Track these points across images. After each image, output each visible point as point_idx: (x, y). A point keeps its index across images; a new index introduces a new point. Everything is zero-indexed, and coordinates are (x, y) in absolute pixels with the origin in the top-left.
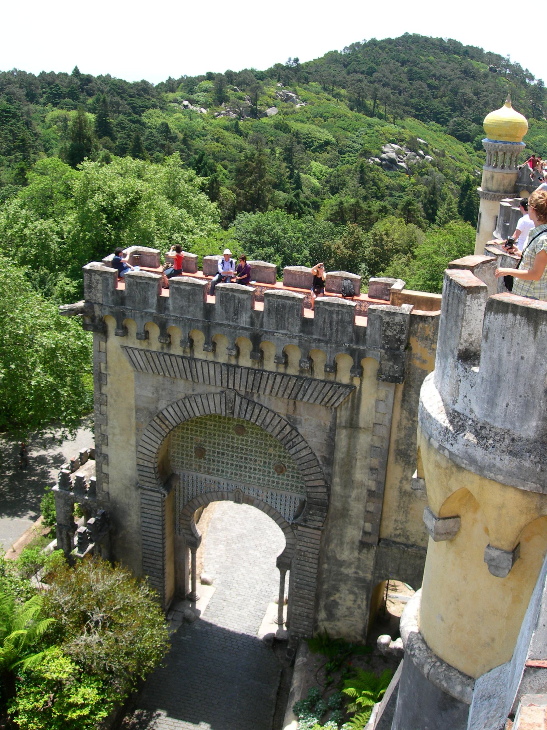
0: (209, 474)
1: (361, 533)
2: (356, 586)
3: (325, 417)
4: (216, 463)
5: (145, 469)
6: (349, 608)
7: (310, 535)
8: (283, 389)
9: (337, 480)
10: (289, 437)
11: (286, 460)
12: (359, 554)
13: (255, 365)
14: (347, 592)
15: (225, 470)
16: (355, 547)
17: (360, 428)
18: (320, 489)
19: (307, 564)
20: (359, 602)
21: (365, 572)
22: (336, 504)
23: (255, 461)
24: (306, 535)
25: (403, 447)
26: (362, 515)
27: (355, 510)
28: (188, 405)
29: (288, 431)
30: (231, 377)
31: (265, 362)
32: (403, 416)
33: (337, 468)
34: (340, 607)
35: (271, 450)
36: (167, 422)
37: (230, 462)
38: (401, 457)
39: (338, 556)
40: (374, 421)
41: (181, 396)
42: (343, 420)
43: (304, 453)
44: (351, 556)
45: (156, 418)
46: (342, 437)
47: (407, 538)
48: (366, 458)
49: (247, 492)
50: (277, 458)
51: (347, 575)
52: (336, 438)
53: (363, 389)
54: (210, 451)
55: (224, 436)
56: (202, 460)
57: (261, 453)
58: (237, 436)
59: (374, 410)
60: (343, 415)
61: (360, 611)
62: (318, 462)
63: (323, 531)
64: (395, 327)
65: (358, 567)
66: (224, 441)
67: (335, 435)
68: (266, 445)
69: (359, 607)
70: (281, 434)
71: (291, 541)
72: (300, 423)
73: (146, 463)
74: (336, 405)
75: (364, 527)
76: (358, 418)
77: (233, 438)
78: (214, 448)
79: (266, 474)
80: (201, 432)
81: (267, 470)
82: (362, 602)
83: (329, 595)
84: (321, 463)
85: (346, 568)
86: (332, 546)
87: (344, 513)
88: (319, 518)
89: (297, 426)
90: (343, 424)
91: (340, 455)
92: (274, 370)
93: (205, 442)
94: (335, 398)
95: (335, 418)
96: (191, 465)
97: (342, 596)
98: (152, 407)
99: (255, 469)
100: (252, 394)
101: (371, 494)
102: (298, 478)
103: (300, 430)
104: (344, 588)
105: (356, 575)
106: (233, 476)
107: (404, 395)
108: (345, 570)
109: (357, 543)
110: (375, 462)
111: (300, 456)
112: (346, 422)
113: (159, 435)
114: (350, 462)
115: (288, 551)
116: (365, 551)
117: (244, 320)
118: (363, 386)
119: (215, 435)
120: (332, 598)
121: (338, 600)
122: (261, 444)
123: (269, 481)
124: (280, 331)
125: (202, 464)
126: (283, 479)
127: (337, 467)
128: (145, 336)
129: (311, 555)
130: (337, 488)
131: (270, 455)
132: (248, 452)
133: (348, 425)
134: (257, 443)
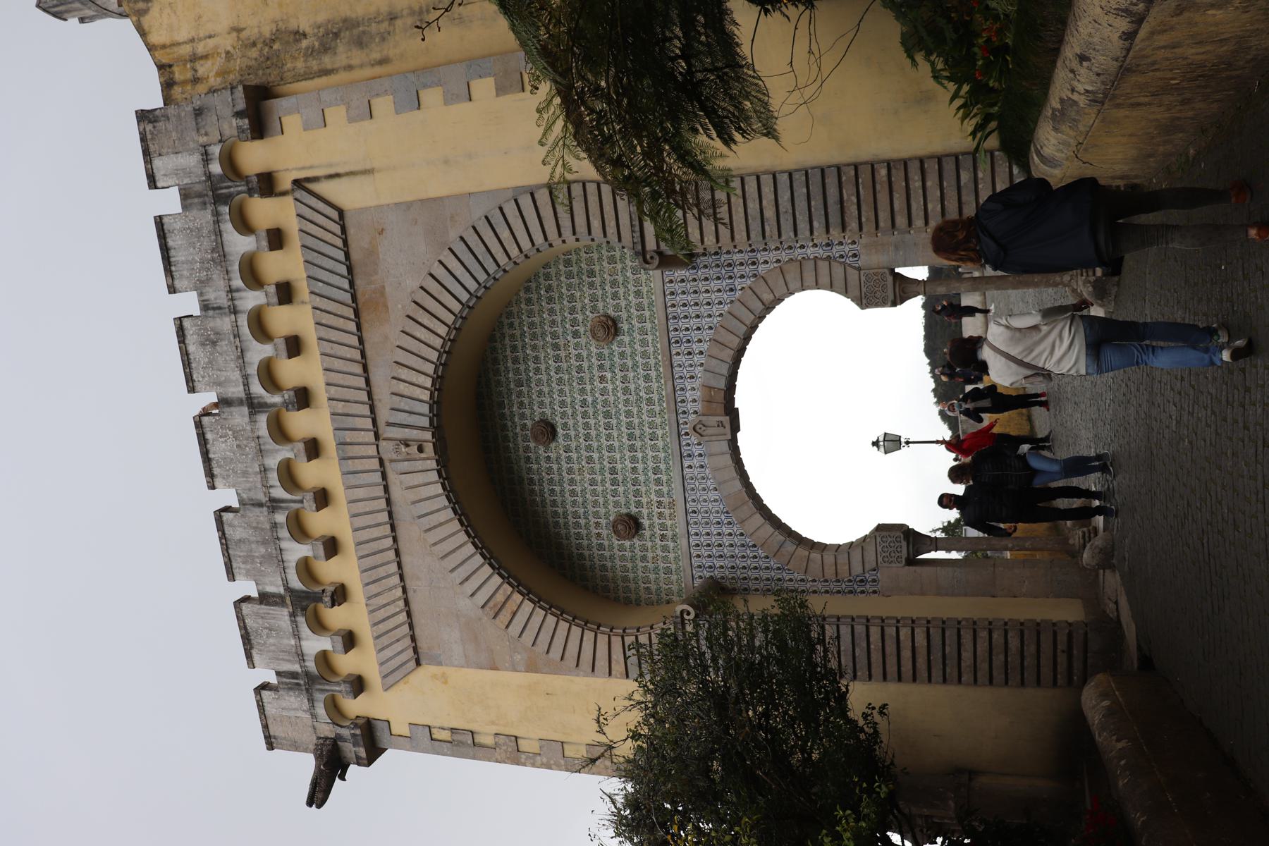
0: (672, 504)
36: (500, 598)
49: (690, 407)
50: (583, 341)
54: (617, 504)
56: (646, 522)
58: (561, 440)
74: (335, 215)
79: (629, 363)
80: (577, 525)
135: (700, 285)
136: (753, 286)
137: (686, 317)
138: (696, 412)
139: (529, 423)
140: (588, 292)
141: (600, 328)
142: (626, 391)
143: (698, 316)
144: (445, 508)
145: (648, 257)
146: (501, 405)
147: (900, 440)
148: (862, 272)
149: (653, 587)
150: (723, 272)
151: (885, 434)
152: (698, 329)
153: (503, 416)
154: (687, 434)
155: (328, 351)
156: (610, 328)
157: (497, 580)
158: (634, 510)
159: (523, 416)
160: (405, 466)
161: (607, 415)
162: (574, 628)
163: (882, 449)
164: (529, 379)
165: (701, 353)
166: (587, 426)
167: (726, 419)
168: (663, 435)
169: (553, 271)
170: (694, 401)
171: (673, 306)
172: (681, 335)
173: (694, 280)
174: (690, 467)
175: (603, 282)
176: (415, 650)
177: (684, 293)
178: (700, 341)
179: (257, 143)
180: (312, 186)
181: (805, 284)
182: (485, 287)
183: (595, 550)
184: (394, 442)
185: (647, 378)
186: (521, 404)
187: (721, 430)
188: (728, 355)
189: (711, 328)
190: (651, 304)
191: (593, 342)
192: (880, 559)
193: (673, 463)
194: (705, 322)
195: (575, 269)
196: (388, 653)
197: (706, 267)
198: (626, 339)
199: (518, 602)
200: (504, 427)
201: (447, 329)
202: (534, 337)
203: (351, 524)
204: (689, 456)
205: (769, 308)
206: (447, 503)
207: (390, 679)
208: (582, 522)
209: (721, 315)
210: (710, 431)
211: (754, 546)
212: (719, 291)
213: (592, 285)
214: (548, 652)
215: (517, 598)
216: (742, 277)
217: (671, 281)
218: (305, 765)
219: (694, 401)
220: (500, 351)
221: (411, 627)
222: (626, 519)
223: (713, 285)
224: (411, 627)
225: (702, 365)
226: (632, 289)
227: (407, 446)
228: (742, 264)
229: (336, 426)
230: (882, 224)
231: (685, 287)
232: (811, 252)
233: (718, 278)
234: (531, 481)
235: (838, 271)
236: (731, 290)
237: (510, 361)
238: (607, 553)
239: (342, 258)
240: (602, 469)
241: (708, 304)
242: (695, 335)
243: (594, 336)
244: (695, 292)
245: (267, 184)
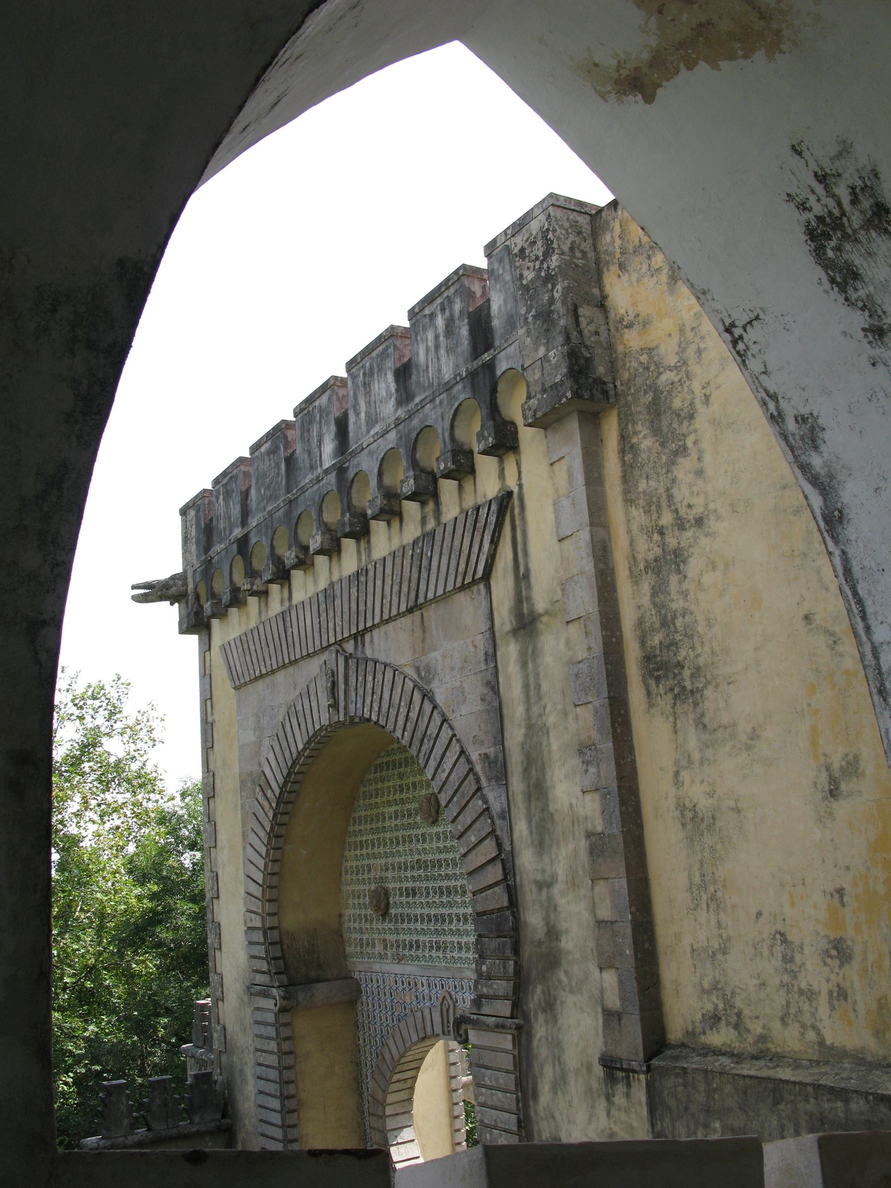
17: (540, 615)
38: (658, 679)
47: (738, 1025)
91: (515, 735)
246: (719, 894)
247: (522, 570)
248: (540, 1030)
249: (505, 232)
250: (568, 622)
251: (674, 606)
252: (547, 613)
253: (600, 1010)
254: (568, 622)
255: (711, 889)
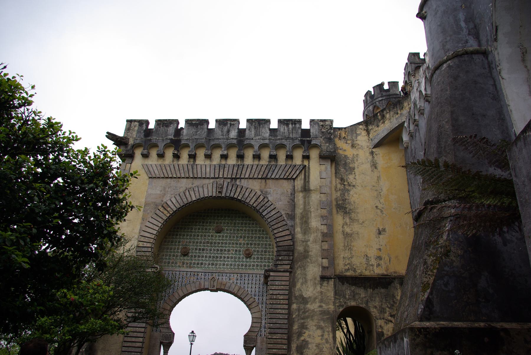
0: (190, 267)
1: (321, 269)
2: (323, 319)
3: (286, 186)
4: (197, 258)
5: (144, 249)
6: (318, 346)
7: (280, 278)
8: (258, 172)
9: (298, 229)
10: (262, 203)
11: (253, 246)
12: (321, 288)
13: (238, 162)
14: (315, 328)
15: (204, 262)
16: (317, 282)
17: (311, 190)
18: (287, 238)
19: (279, 306)
20: (326, 336)
21: (327, 304)
22: (300, 248)
23: (229, 251)
24: (277, 278)
25: (341, 202)
26: (320, 254)
27: (314, 251)
28: (187, 193)
29: (261, 199)
30: (222, 170)
31: (245, 159)
32: (337, 182)
33: (298, 221)
34: (310, 346)
35: (241, 241)
36: (169, 209)
37: (208, 255)
38: (340, 209)
39: (304, 294)
40: (320, 184)
41: (182, 190)
42: (300, 187)
43: (273, 213)
44: (314, 292)
45: (160, 207)
46: (300, 198)
47: (355, 271)
48: (318, 210)
50: (245, 246)
51: (313, 311)
52: (295, 200)
53: (310, 166)
55: (205, 236)
56: (185, 258)
57: (233, 244)
59: (319, 178)
60: (299, 183)
61: (328, 346)
62: (284, 218)
63: (291, 272)
64: (326, 127)
65: (321, 301)
66: (205, 239)
67: (294, 197)
68: (237, 237)
69: (327, 342)
70: (256, 202)
71: (257, 315)
72: (270, 193)
73: (145, 245)
74: (294, 177)
75: (322, 263)
76: (309, 184)
77: (212, 236)
78: (197, 246)
79: (237, 260)
80: (187, 235)
81: (238, 256)
82: (329, 335)
83: (300, 334)
84: (285, 218)
85: (311, 304)
86: (298, 286)
87: (306, 255)
88: (286, 262)
89: (267, 196)
90: (300, 190)
91: (299, 211)
92: (252, 163)
93: (190, 242)
94: (293, 172)
95: (294, 187)
96: (176, 263)
97: (311, 333)
98: (158, 201)
99: (228, 258)
100: (236, 179)
101: (324, 235)
102: (261, 258)
103: (270, 199)
104: (311, 324)
105: (320, 309)
106: (210, 266)
107: (336, 170)
108: (311, 306)
109: (318, 279)
110: (324, 212)
111: (270, 216)
112: (301, 187)
113: (160, 220)
114: (307, 214)
115: (255, 325)
116: (325, 284)
117: (233, 134)
118: (310, 164)
119: (198, 236)
120: (302, 338)
121: (308, 339)
122: (234, 237)
123: (239, 265)
124: (257, 137)
125: (186, 261)
126: (250, 262)
127: (297, 220)
128: (161, 156)
129: (282, 297)
130: (299, 236)
131: (240, 244)
132: (223, 245)
133: (303, 190)
134: (230, 237)
135: (258, 285)
136: (255, 302)
137: (248, 280)
138: (219, 279)
139: (222, 225)
140: (260, 250)
141: (249, 252)
142: (228, 258)
143: (248, 283)
144: (200, 196)
145: (268, 273)
146: (229, 217)
147: (193, 341)
148: (255, 337)
149: (164, 257)
150: (261, 293)
151: (196, 336)
152: (244, 283)
153: (225, 217)
154: (212, 275)
155: (254, 167)
156: (248, 255)
157: (175, 209)
158: (190, 254)
159: (224, 223)
160: (215, 185)
161: (221, 250)
162: (156, 232)
163: (191, 334)
164: (236, 227)
165: (237, 283)
166: (219, 243)
167: (215, 288)
168: (213, 267)
169: (268, 240)
170: (222, 279)
171: (252, 276)
172: (243, 278)
173: (259, 284)
174: (202, 275)
175: (262, 255)
176: (154, 178)
177: (256, 280)
178: (241, 283)
179: (318, 156)
180: (303, 172)
181: (254, 319)
182: (266, 221)
183: (179, 240)
184: (223, 184)
185: (231, 265)
186: (228, 223)
187: (212, 286)
188: (235, 291)
189: (244, 287)
190: (254, 269)
191: (245, 249)
192: (164, 333)
193: (203, 270)
194: (246, 285)
195: (268, 247)
196: (155, 168)
197: (263, 288)
198: (244, 260)
199: (167, 215)
200: (222, 217)
201: (255, 207)
202: (249, 231)
203: (199, 164)
204: (205, 275)
205: (248, 306)
206: (201, 197)
207: (145, 166)
208: (188, 237)
209: (248, 291)
210: (212, 282)
211: (173, 292)
212: (255, 291)
213: (262, 251)
214: (148, 221)
215: (168, 215)
216: (259, 299)
217: (260, 276)
218: (120, 133)
219: (222, 279)
220: (246, 219)
221: (162, 178)
222: (188, 252)
223: (257, 289)
224: (162, 178)
225: (233, 283)
226: (259, 264)
227: (221, 188)
228: (262, 299)
229: (230, 165)
230: (269, 345)
231: (258, 281)
232: (263, 322)
233: (259, 291)
234: (203, 223)
235: (256, 330)
236: (255, 295)
237: (242, 222)
238: (177, 244)
239: (281, 177)
240: (204, 246)
241: (252, 287)
242: (242, 282)
243: (247, 250)
244: (256, 284)
245: (306, 157)
246: (352, 248)
247: (307, 180)
248: (299, 272)
249: (318, 120)
250: (321, 193)
251: (346, 198)
252: (314, 190)
253: (321, 267)
254: (321, 193)
255: (350, 247)
